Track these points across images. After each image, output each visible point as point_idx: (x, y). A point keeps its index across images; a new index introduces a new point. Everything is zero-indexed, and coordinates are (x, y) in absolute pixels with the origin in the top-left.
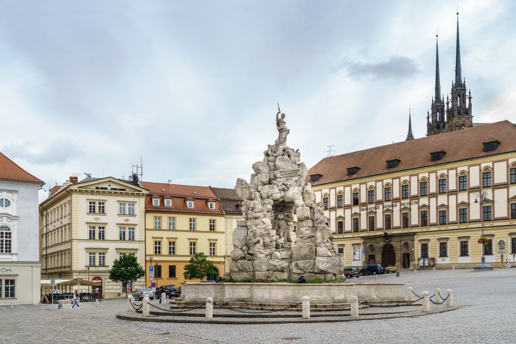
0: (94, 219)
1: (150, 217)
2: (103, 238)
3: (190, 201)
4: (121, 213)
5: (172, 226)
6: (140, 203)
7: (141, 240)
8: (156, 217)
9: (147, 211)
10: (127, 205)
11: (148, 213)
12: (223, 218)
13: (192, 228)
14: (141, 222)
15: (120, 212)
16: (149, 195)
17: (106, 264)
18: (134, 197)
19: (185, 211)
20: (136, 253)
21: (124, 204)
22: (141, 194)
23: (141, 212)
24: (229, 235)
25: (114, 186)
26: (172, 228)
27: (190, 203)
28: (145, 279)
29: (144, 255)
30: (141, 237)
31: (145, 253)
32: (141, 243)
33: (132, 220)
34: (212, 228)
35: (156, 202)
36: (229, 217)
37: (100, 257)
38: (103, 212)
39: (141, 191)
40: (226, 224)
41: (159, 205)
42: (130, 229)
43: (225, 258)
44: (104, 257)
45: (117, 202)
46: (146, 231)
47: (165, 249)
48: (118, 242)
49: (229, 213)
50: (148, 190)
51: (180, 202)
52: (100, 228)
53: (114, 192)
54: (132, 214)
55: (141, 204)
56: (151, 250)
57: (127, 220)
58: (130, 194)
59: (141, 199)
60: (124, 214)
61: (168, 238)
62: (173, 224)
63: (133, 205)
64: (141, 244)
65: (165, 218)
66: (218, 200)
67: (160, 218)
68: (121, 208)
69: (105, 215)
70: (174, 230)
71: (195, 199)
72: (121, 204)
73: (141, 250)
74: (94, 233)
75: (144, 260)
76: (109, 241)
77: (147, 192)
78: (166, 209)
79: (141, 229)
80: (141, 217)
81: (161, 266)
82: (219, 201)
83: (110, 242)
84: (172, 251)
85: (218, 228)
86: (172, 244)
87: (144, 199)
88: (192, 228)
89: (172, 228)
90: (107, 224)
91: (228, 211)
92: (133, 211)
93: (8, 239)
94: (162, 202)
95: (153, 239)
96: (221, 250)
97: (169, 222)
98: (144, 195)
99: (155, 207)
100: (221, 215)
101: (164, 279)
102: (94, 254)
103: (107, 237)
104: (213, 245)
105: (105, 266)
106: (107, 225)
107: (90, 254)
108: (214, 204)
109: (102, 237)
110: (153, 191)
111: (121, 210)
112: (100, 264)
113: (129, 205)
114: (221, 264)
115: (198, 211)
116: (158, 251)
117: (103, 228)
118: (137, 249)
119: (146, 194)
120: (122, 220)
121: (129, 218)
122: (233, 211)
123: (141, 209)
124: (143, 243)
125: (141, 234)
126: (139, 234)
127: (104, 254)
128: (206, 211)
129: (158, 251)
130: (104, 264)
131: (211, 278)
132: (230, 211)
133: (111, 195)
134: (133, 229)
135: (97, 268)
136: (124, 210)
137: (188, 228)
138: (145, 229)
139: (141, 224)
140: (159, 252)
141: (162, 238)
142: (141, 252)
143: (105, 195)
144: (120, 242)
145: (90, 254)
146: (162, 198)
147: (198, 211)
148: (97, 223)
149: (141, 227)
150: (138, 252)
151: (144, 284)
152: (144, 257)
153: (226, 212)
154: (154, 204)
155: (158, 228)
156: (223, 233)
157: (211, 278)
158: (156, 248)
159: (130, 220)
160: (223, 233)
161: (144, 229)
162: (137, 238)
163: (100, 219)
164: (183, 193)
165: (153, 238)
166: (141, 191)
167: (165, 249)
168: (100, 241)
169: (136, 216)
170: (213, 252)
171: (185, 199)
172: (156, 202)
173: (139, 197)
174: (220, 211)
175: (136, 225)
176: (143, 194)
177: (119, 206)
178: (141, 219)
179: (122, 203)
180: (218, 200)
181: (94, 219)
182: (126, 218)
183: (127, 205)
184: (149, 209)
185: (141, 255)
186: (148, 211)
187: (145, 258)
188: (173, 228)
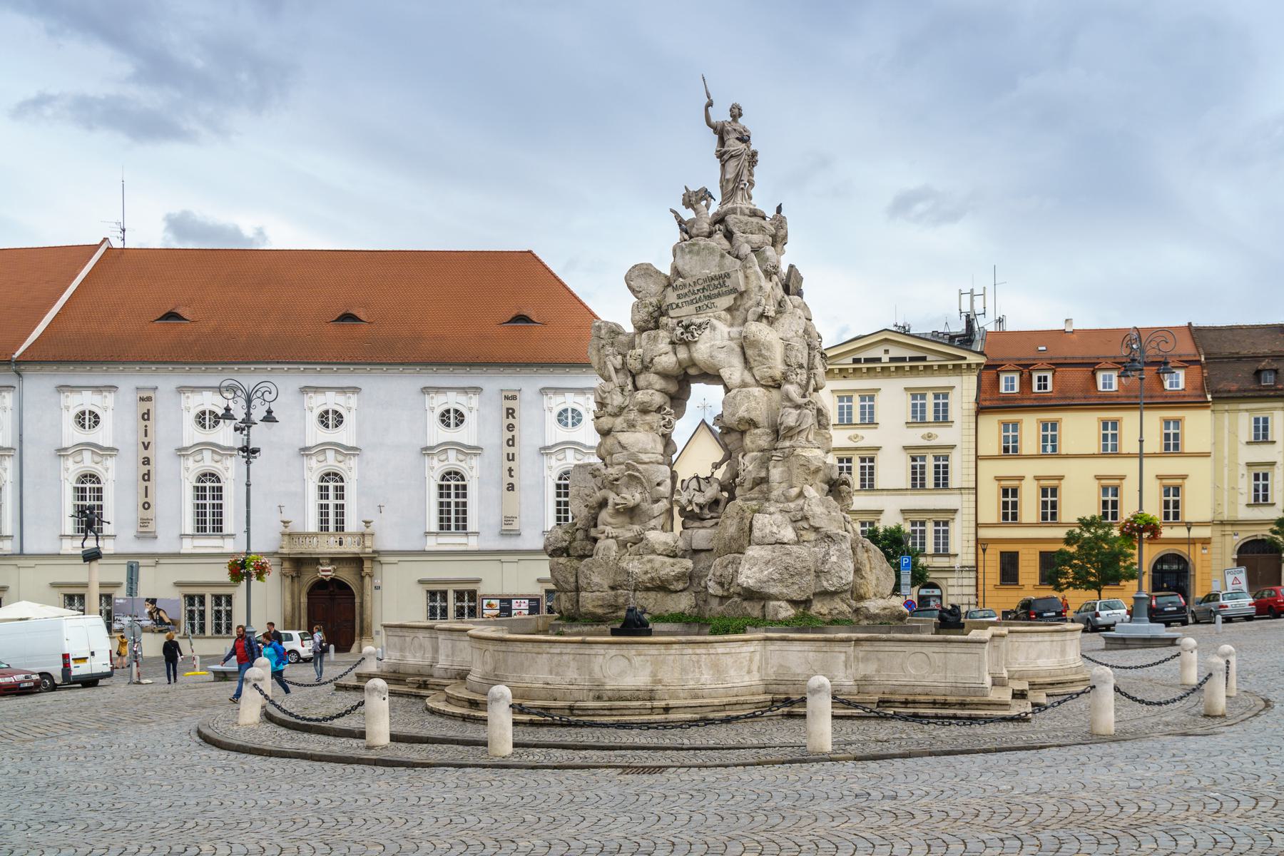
0: (850, 438)
1: (991, 426)
2: (871, 486)
3: (1107, 373)
4: (915, 420)
5: (1049, 443)
6: (964, 390)
7: (965, 485)
8: (1006, 425)
9: (981, 410)
10: (856, 399)
11: (984, 413)
12: (1208, 412)
13: (1110, 449)
14: (965, 439)
15: (913, 417)
16: (988, 367)
17: (951, 551)
18: (947, 374)
19: (1091, 401)
20: (953, 519)
21: (923, 397)
22: (964, 367)
23: (966, 413)
24: (1226, 461)
25: (896, 352)
26: (1050, 447)
27: (1104, 378)
28: (974, 589)
29: (973, 524)
30: (965, 478)
31: (974, 519)
32: (965, 494)
33: (943, 435)
34: (1172, 445)
35: (1009, 383)
36: (1226, 407)
37: (937, 532)
38: (945, 417)
39: (965, 358)
40: (1217, 429)
41: (1017, 389)
42: (937, 458)
43: (1189, 529)
44: (946, 532)
45: (904, 393)
46: (979, 462)
47: (1030, 507)
48: (905, 495)
49: (1223, 397)
50: (981, 353)
51: (1076, 377)
52: (863, 460)
53: (899, 367)
54: (942, 417)
55: (965, 393)
56: (991, 510)
57: (929, 436)
58: (936, 368)
59: (965, 378)
60: (923, 422)
61: (1037, 478)
62: (1054, 439)
63: (946, 396)
64: (965, 497)
65: (1030, 426)
66: (1198, 362)
67: (1016, 425)
68: (914, 406)
69: (876, 428)
70: (1056, 455)
71: (1056, 366)
72: (914, 397)
73: (965, 511)
74: (923, 473)
75: (973, 537)
76: (885, 493)
77: (982, 360)
78: (1035, 399)
79: (965, 458)
80: (966, 426)
81: (1018, 553)
82: (1201, 364)
83: (887, 495)
84: (1050, 513)
85: (1188, 445)
86: (1050, 494)
87: (974, 379)
88: (1110, 449)
89: (1049, 449)
90: (878, 449)
91: (1225, 391)
92: (945, 411)
93: (563, 499)
94: (1026, 383)
95: (997, 483)
96: (1196, 506)
97: (1042, 433)
98: (973, 366)
99: (1006, 398)
100: (1200, 404)
101: (1026, 587)
102: (923, 524)
103: (878, 485)
104: (1173, 492)
105: (949, 556)
106: (879, 453)
107: (935, 526)
108: (1181, 374)
109: (942, 481)
110: (997, 354)
111: (914, 412)
112: (937, 550)
113: (937, 396)
114: (1199, 546)
115: (1129, 397)
116: (1010, 513)
117: (872, 460)
118: (955, 511)
119: (978, 365)
120: (916, 436)
121: (860, 432)
122: (1239, 390)
123: (965, 406)
124: (969, 494)
125: (965, 471)
126: (959, 473)
127: (946, 524)
128: (1151, 397)
129: (1010, 513)
130: (946, 550)
131: (1165, 585)
132: (1229, 391)
133: (889, 376)
134: (946, 458)
135: (929, 559)
136: (923, 412)
137: (1095, 448)
138: (977, 457)
139: (966, 445)
140: (1015, 517)
141: (1021, 478)
142: (965, 517)
143: (876, 377)
144: (911, 494)
145: (935, 526)
146: (1025, 369)
147: (1129, 397)
148: (856, 449)
149: (965, 452)
150: (958, 516)
151: (973, 599)
152: (973, 530)
153: (1216, 395)
154: (1002, 390)
155: (1010, 450)
156: (1206, 455)
157: (1165, 585)
158: (1005, 505)
159: (937, 436)
160: (1206, 455)
161: (973, 458)
162: (954, 481)
163: (863, 438)
164: (1079, 353)
165: (998, 479)
166: (965, 358)
167: (1030, 507)
168: (863, 493)
169: (954, 425)
170: (1173, 511)
171: (1092, 366)
172: (1009, 383)
173: (961, 374)
174: (1199, 392)
175: (953, 447)
176: (969, 365)
177: (910, 401)
178: (966, 432)
179: (917, 394)
180: (1199, 361)
181: (850, 438)
182: (852, 432)
183: (856, 399)
184: (987, 404)
185: (966, 524)
186: (982, 408)
187: (974, 532)
188: (1115, 447)
